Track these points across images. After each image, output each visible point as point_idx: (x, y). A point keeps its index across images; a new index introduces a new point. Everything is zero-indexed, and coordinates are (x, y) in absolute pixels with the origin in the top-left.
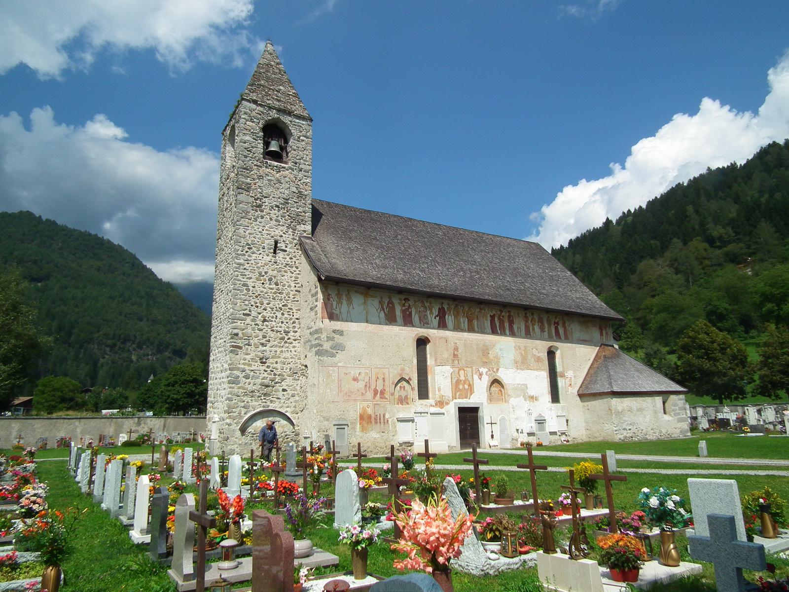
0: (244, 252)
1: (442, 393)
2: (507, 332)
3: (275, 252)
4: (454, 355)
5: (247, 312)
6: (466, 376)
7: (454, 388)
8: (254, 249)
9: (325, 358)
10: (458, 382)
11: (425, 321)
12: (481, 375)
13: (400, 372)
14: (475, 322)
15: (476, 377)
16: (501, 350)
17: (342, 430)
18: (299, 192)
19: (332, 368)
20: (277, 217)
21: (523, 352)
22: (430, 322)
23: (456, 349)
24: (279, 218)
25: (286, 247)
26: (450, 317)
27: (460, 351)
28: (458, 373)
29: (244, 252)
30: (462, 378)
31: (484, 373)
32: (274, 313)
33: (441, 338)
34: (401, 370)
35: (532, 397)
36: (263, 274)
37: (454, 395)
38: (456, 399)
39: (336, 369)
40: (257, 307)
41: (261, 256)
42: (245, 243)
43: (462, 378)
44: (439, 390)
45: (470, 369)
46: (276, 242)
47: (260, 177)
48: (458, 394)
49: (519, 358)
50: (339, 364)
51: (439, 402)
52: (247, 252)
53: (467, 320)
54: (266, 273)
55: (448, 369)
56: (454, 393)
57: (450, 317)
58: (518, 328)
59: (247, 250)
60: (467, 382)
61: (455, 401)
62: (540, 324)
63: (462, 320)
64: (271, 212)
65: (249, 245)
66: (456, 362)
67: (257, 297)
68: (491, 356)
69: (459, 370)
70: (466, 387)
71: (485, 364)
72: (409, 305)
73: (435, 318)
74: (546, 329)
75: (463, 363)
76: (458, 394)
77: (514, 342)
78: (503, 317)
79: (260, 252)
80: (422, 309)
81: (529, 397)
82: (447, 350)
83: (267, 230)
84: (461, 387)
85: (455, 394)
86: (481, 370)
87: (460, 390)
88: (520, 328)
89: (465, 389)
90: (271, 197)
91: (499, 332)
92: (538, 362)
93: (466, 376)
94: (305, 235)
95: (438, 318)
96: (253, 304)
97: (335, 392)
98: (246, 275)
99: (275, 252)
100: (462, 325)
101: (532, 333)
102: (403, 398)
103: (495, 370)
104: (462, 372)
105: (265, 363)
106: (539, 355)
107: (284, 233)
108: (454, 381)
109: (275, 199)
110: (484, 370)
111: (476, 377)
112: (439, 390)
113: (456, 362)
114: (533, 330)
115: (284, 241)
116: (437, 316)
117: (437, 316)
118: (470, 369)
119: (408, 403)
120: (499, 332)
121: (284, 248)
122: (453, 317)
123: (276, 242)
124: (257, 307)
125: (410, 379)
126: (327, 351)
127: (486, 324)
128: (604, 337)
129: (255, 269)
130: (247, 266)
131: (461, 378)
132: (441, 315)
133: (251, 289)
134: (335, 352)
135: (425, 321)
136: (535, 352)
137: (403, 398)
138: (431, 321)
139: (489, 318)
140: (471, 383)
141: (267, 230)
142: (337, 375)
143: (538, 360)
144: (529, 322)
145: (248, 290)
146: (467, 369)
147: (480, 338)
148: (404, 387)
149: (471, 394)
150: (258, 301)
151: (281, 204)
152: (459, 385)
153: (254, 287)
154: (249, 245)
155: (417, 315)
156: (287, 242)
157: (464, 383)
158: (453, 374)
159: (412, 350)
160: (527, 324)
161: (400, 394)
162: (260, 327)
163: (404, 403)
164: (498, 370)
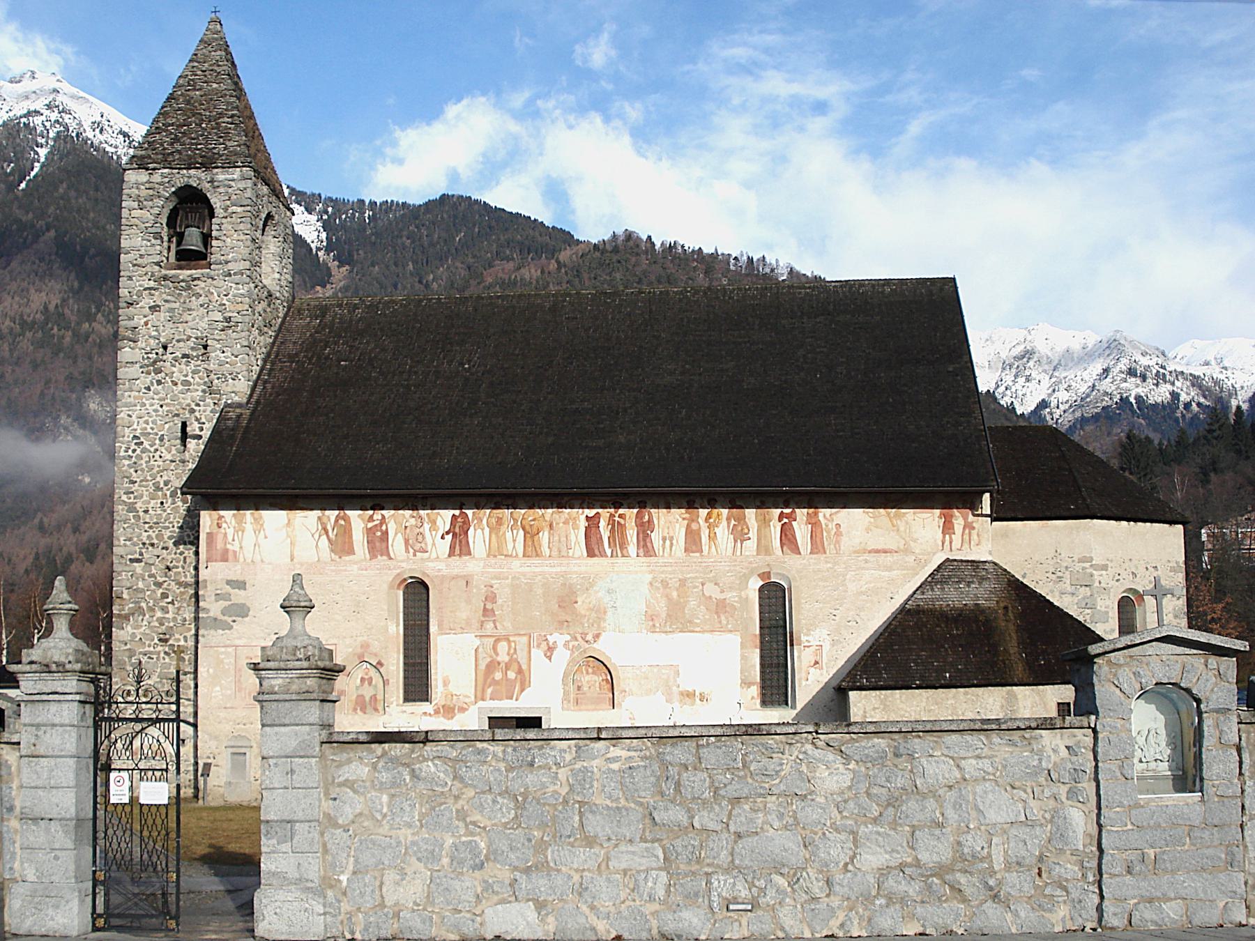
0: (130, 453)
1: (452, 688)
2: (632, 549)
3: (184, 443)
4: (485, 609)
5: (137, 556)
6: (512, 653)
7: (481, 679)
8: (146, 444)
9: (212, 632)
10: (492, 666)
11: (418, 546)
12: (550, 650)
13: (359, 650)
14: (544, 537)
15: (538, 654)
16: (609, 591)
17: (241, 758)
18: (225, 318)
19: (223, 649)
20: (186, 376)
21: (675, 594)
22: (429, 549)
23: (491, 598)
24: (189, 378)
25: (201, 429)
26: (479, 531)
27: (500, 601)
28: (494, 648)
29: (130, 453)
30: (503, 657)
31: (560, 644)
32: (181, 554)
33: (454, 578)
34: (362, 646)
35: (690, 695)
36: (162, 485)
37: (479, 694)
38: (483, 699)
39: (230, 649)
40: (152, 545)
41: (158, 453)
42: (131, 436)
43: (503, 657)
44: (446, 683)
45: (525, 639)
46: (184, 425)
47: (155, 309)
48: (489, 691)
49: (662, 607)
50: (237, 642)
51: (443, 706)
52: (134, 451)
53: (521, 532)
54: (166, 483)
55: (469, 641)
56: (479, 688)
57: (479, 531)
58: (664, 539)
59: (133, 447)
60: (515, 666)
61: (481, 704)
62: (733, 522)
63: (509, 535)
64: (174, 369)
65: (139, 438)
66: (490, 625)
67: (151, 527)
68: (581, 607)
69: (497, 641)
70: (511, 675)
71: (562, 625)
72: (383, 516)
73: (443, 538)
74: (753, 534)
75: (506, 626)
76: (489, 691)
77: (650, 572)
78: (620, 516)
79: (155, 447)
80: (413, 521)
81: (682, 694)
82: (468, 601)
83: (167, 405)
84: (498, 676)
85: (483, 691)
86: (551, 639)
87: (495, 682)
88: (671, 539)
89: (507, 680)
90: (174, 342)
91: (609, 552)
92: (717, 613)
93: (512, 653)
94: (237, 399)
95: (449, 538)
96: (145, 540)
97: (229, 692)
98: (132, 493)
99: (184, 443)
100: (510, 546)
101: (705, 548)
102: (367, 699)
103: (589, 637)
104: (503, 646)
105: (166, 641)
106: (722, 596)
107: (198, 405)
108: (482, 666)
109: (182, 344)
110: (559, 638)
111: (538, 654)
112: (446, 683)
113: (490, 625)
114: (712, 537)
115: (197, 420)
116: (448, 533)
117: (448, 533)
118: (525, 639)
119: (376, 710)
120: (609, 552)
121: (198, 432)
122: (487, 530)
123: (184, 425)
124: (152, 545)
125: (380, 663)
126: (216, 619)
127: (573, 537)
128: (957, 538)
129: (149, 478)
130: (134, 477)
131: (499, 659)
132: (457, 530)
133: (141, 514)
134: (229, 620)
135: (418, 546)
136: (711, 590)
137: (367, 699)
138: (434, 544)
139: (583, 523)
140: (524, 667)
141: (167, 405)
142: (233, 661)
143: (721, 607)
144: (700, 520)
145: (137, 518)
146: (516, 639)
147: (554, 570)
148: (371, 679)
149: (522, 690)
150: (154, 535)
151: (192, 349)
152: (493, 672)
153: (146, 512)
154: (139, 438)
155: (400, 537)
156: (203, 420)
157: (508, 666)
158: (480, 650)
159: (386, 607)
160: (694, 526)
161: (360, 692)
162: (160, 580)
163: (369, 709)
164: (597, 636)
